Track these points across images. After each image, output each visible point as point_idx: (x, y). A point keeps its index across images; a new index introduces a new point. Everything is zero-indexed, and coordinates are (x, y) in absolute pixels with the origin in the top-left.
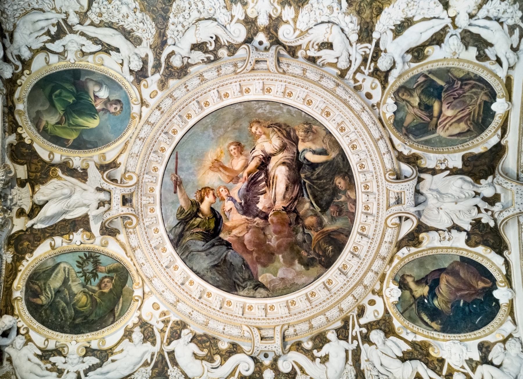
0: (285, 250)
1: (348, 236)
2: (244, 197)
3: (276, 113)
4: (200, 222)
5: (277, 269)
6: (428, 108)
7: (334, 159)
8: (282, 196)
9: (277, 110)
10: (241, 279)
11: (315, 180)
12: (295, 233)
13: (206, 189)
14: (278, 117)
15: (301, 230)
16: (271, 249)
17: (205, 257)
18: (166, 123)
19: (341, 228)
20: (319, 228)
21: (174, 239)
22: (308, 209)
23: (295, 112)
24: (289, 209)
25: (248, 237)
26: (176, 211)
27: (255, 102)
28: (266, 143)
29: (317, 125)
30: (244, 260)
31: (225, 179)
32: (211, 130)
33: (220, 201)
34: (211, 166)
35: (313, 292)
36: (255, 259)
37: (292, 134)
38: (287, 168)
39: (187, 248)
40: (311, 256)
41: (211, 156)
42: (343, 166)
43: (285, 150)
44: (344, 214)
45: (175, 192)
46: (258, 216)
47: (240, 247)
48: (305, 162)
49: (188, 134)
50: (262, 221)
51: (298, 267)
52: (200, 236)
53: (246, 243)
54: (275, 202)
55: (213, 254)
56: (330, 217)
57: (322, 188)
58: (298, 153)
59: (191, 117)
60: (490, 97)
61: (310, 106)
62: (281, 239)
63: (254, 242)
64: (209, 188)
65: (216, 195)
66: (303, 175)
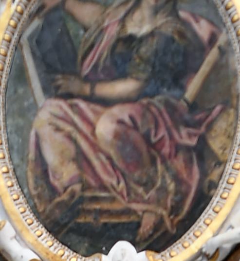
6: (117, 69)
60: (151, 236)
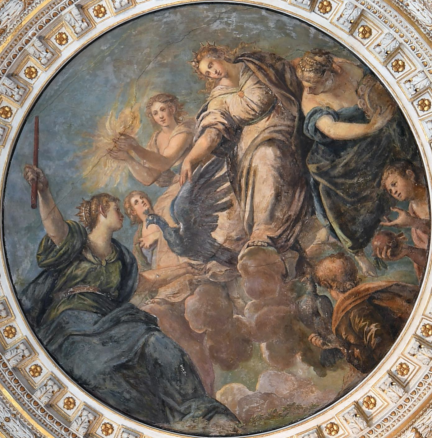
0: (275, 333)
1: (411, 301)
2: (183, 215)
3: (252, 30)
4: (89, 272)
5: (257, 374)
7: (381, 130)
8: (268, 213)
9: (255, 23)
10: (177, 396)
11: (339, 177)
12: (295, 295)
13: (102, 199)
14: (257, 38)
15: (309, 288)
16: (244, 330)
17: (100, 347)
18: (11, 55)
19: (397, 285)
20: (348, 285)
21: (33, 308)
22: (323, 243)
23: (295, 26)
24: (281, 242)
25: (192, 302)
26: (37, 247)
27: (206, 7)
28: (230, 96)
29: (345, 57)
30: (183, 354)
31: (142, 176)
32: (110, 68)
33: (132, 224)
34: (111, 147)
35: (333, 424)
36: (207, 353)
37: (288, 76)
38: (278, 152)
39: (60, 328)
40: (331, 346)
41: (111, 126)
42: (402, 146)
43: (274, 112)
44: (404, 252)
45: (35, 206)
46: (213, 257)
47: (175, 325)
48: (317, 138)
49: (60, 78)
50: (224, 269)
51: (302, 369)
52: (89, 302)
53: (187, 316)
54: (251, 227)
55: (117, 342)
56: (372, 259)
57: (355, 195)
58: (302, 117)
59: (67, 39)
61: (326, 15)
62: (265, 309)
63: (205, 314)
64: (106, 195)
65: (122, 211)
66: (312, 168)
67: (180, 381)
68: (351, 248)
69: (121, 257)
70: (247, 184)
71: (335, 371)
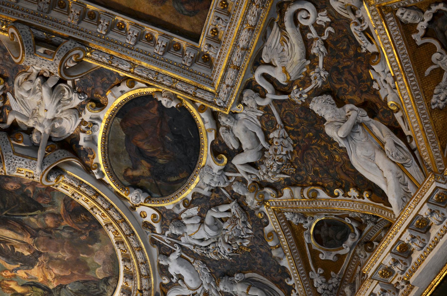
15: (58, 231)
53: (62, 274)
54: (24, 242)
63: (63, 269)
67: (90, 287)
68: (42, 211)
69: (31, 286)
70: (3, 238)
71: (99, 236)
